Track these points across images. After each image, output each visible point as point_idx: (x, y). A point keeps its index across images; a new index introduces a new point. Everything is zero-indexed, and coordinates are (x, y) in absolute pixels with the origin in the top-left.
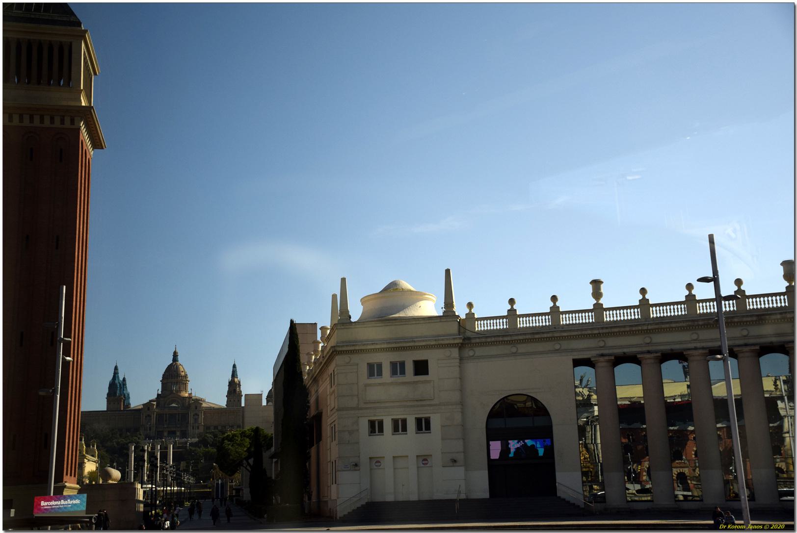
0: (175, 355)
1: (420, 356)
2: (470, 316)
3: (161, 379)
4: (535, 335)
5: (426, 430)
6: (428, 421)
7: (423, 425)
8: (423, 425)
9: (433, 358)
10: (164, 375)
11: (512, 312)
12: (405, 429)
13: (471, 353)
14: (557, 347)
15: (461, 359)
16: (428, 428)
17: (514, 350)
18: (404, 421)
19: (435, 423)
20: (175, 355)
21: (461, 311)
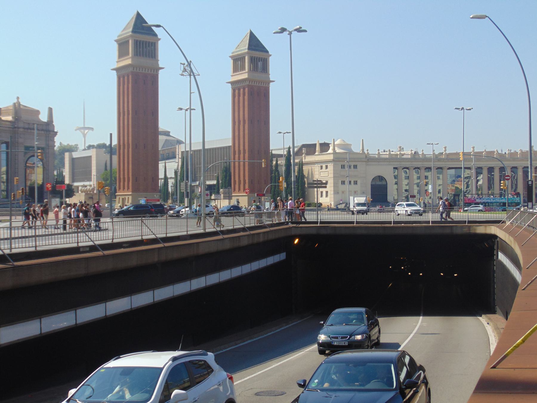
1: (355, 163)
2: (368, 153)
4: (385, 160)
7: (356, 183)
8: (356, 183)
9: (358, 164)
11: (379, 153)
19: (359, 182)
21: (366, 152)
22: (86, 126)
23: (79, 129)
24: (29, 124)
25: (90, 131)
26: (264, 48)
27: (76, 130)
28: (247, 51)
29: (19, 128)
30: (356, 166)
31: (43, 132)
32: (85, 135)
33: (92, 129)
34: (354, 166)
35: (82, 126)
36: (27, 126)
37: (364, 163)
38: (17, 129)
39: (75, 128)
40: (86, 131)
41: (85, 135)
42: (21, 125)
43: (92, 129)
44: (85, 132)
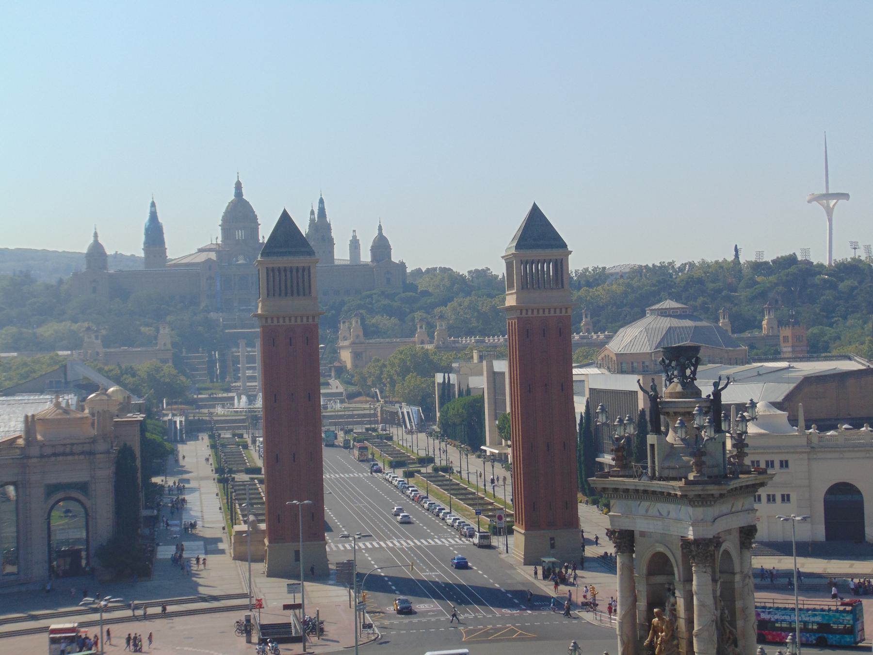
0: (238, 186)
1: (784, 457)
3: (220, 223)
5: (787, 501)
6: (788, 496)
7: (786, 498)
8: (786, 498)
10: (224, 219)
12: (774, 500)
13: (815, 456)
14: (868, 455)
15: (809, 459)
16: (788, 500)
17: (841, 456)
18: (774, 496)
20: (238, 186)
22: (830, 192)
23: (818, 198)
24: (53, 446)
25: (842, 202)
26: (559, 238)
27: (809, 202)
28: (514, 252)
29: (29, 457)
30: (787, 462)
31: (82, 457)
32: (829, 212)
33: (846, 196)
34: (781, 462)
35: (824, 192)
36: (48, 451)
37: (805, 456)
38: (25, 461)
39: (808, 198)
40: (832, 203)
41: (829, 212)
42: (34, 451)
43: (846, 196)
44: (831, 205)
